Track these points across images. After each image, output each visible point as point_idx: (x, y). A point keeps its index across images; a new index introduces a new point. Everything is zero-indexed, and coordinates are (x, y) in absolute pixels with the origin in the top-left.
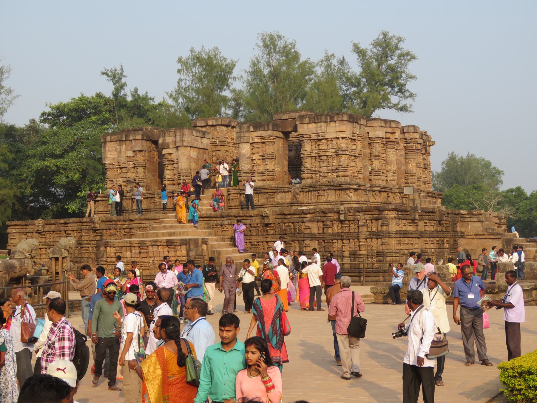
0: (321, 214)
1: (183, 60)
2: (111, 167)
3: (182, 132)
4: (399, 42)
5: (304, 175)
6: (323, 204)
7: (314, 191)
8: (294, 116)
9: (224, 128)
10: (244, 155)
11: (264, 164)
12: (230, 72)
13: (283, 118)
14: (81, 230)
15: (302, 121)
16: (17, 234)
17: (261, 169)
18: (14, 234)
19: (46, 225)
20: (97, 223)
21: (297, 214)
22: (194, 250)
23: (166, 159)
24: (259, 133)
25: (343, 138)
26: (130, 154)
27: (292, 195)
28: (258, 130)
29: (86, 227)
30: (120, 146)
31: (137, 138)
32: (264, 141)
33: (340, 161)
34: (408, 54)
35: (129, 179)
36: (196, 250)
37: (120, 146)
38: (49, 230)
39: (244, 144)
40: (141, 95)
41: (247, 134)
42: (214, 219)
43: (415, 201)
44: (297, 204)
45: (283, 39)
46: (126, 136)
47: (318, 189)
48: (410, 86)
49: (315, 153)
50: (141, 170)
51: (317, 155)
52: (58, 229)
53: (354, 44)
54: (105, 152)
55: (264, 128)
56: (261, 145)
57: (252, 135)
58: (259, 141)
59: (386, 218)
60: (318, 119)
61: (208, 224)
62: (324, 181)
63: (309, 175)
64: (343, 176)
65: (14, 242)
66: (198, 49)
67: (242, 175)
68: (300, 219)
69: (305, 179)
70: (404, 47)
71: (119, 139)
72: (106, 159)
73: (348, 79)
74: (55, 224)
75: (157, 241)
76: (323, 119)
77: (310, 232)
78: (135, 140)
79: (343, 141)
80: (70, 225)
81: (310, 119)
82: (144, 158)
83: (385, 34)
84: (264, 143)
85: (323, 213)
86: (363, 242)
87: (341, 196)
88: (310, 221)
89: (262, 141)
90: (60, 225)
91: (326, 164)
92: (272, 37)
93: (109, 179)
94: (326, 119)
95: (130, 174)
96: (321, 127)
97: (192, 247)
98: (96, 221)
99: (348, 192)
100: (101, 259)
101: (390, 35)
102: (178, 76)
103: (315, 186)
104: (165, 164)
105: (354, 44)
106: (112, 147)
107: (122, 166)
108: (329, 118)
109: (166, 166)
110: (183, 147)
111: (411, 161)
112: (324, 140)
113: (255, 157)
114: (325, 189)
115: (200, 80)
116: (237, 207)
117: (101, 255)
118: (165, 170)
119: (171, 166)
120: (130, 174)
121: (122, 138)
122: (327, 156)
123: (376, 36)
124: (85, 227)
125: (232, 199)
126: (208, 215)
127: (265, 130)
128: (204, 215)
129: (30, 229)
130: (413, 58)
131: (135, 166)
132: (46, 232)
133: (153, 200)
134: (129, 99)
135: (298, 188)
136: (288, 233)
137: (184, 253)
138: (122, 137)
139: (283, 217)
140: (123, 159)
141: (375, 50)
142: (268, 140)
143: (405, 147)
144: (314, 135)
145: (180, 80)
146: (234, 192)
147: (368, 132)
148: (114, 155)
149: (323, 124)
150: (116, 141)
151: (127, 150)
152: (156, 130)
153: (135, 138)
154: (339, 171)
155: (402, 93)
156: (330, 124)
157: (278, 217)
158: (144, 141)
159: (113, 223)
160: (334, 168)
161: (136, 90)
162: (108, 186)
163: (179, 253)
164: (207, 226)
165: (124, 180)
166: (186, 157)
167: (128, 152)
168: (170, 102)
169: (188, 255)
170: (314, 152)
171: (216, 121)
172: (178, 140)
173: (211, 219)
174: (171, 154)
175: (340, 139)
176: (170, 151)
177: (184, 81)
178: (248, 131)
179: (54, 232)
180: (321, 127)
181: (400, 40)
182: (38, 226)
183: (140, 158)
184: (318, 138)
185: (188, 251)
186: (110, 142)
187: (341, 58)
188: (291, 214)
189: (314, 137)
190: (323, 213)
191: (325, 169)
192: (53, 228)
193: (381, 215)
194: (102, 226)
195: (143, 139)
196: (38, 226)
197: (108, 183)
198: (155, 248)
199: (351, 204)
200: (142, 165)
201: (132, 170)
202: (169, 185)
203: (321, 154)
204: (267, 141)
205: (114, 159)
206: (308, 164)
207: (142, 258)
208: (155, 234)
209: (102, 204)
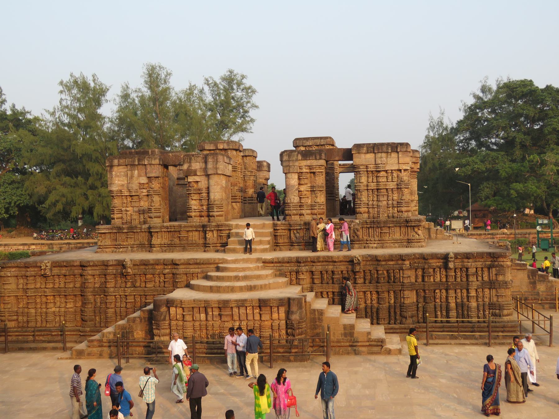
0: (420, 260)
1: (65, 82)
2: (118, 194)
3: (215, 158)
4: (243, 79)
6: (389, 242)
7: (378, 227)
8: (319, 142)
9: (234, 152)
10: (293, 186)
11: (314, 196)
12: (104, 95)
13: (305, 145)
14: (105, 275)
15: (360, 150)
16: (13, 278)
17: (310, 201)
18: (10, 278)
19: (54, 267)
20: (130, 267)
21: (392, 260)
22: (298, 312)
23: (192, 188)
24: (308, 162)
25: (404, 170)
26: (144, 180)
27: (352, 232)
28: (308, 159)
29: (113, 272)
30: (132, 170)
31: (153, 162)
32: (314, 171)
33: (403, 195)
34: (249, 88)
35: (142, 208)
36: (300, 313)
37: (132, 170)
38: (59, 274)
39: (293, 174)
40: (19, 110)
41: (297, 164)
42: (288, 265)
43: (431, 230)
44: (358, 242)
45: (165, 70)
46: (139, 160)
47: (382, 225)
48: (252, 113)
49: (373, 186)
50: (156, 199)
51: (375, 188)
52: (71, 273)
53: (205, 78)
54: (112, 177)
55: (315, 157)
56: (309, 175)
57: (300, 163)
58: (308, 171)
59: (502, 266)
60: (378, 149)
61: (280, 270)
62: (383, 217)
63: (367, 209)
65: (9, 287)
66: (77, 75)
67: (292, 209)
68: (397, 266)
69: (361, 213)
70: (247, 82)
71: (130, 163)
72: (113, 185)
73: (205, 105)
74: (67, 267)
75: (245, 300)
76: (385, 149)
77: (409, 281)
78: (150, 164)
79: (405, 173)
80: (89, 268)
81: (367, 148)
82: (159, 186)
84: (314, 173)
85: (424, 259)
86: (473, 293)
87: (407, 233)
88: (410, 269)
89: (312, 171)
90: (73, 268)
92: (153, 68)
93: (117, 208)
94: (388, 149)
95: (142, 203)
96: (381, 158)
97: (294, 308)
98: (128, 265)
99: (416, 230)
100: (162, 322)
101: (235, 72)
102: (59, 97)
103: (379, 223)
104: (191, 194)
105: (205, 78)
106: (120, 172)
107: (134, 194)
108: (390, 149)
109: (192, 195)
110: (216, 176)
112: (383, 172)
113: (302, 188)
115: (78, 100)
116: (285, 244)
117: (162, 318)
118: (190, 200)
119: (198, 195)
120: (142, 203)
121: (134, 162)
122: (387, 189)
123: (224, 72)
124: (111, 271)
125: (280, 235)
126: (280, 260)
127: (316, 159)
128: (275, 260)
129: (32, 272)
130: (254, 92)
131: (149, 194)
132: (54, 276)
133: (177, 235)
134: (9, 112)
135: (358, 224)
136: (383, 282)
137: (283, 315)
138: (134, 162)
139: (376, 263)
140: (135, 186)
141: (223, 83)
142: (319, 171)
144: (372, 166)
145: (61, 99)
146: (283, 228)
148: (123, 181)
149: (384, 155)
150: (126, 165)
151: (139, 176)
152: (171, 154)
153: (150, 162)
155: (244, 118)
156: (390, 155)
157: (368, 263)
158: (160, 166)
159: (150, 267)
160: (395, 203)
161: (14, 106)
162: (116, 216)
163: (275, 316)
164: (278, 273)
165: (136, 209)
166: (219, 187)
167: (141, 178)
168: (48, 117)
169: (287, 318)
170: (372, 184)
171: (228, 145)
172: (211, 167)
173: (283, 265)
174: (197, 182)
175: (402, 171)
176: (197, 178)
177: (65, 100)
178: (297, 160)
179: (65, 276)
180: (382, 158)
181: (243, 77)
182: (45, 269)
183: (156, 185)
184: (378, 169)
185: (288, 313)
186: (119, 165)
187: (201, 88)
188: (383, 261)
189: (372, 168)
190: (424, 259)
192: (64, 271)
193: (496, 263)
194: (134, 271)
195: (159, 164)
196: (45, 269)
197: (116, 212)
198: (242, 310)
199: (419, 242)
200: (159, 193)
201: (145, 198)
202: (195, 216)
203: (380, 187)
204: (318, 171)
205: (123, 185)
206: (364, 197)
208: (230, 288)
209: (109, 236)
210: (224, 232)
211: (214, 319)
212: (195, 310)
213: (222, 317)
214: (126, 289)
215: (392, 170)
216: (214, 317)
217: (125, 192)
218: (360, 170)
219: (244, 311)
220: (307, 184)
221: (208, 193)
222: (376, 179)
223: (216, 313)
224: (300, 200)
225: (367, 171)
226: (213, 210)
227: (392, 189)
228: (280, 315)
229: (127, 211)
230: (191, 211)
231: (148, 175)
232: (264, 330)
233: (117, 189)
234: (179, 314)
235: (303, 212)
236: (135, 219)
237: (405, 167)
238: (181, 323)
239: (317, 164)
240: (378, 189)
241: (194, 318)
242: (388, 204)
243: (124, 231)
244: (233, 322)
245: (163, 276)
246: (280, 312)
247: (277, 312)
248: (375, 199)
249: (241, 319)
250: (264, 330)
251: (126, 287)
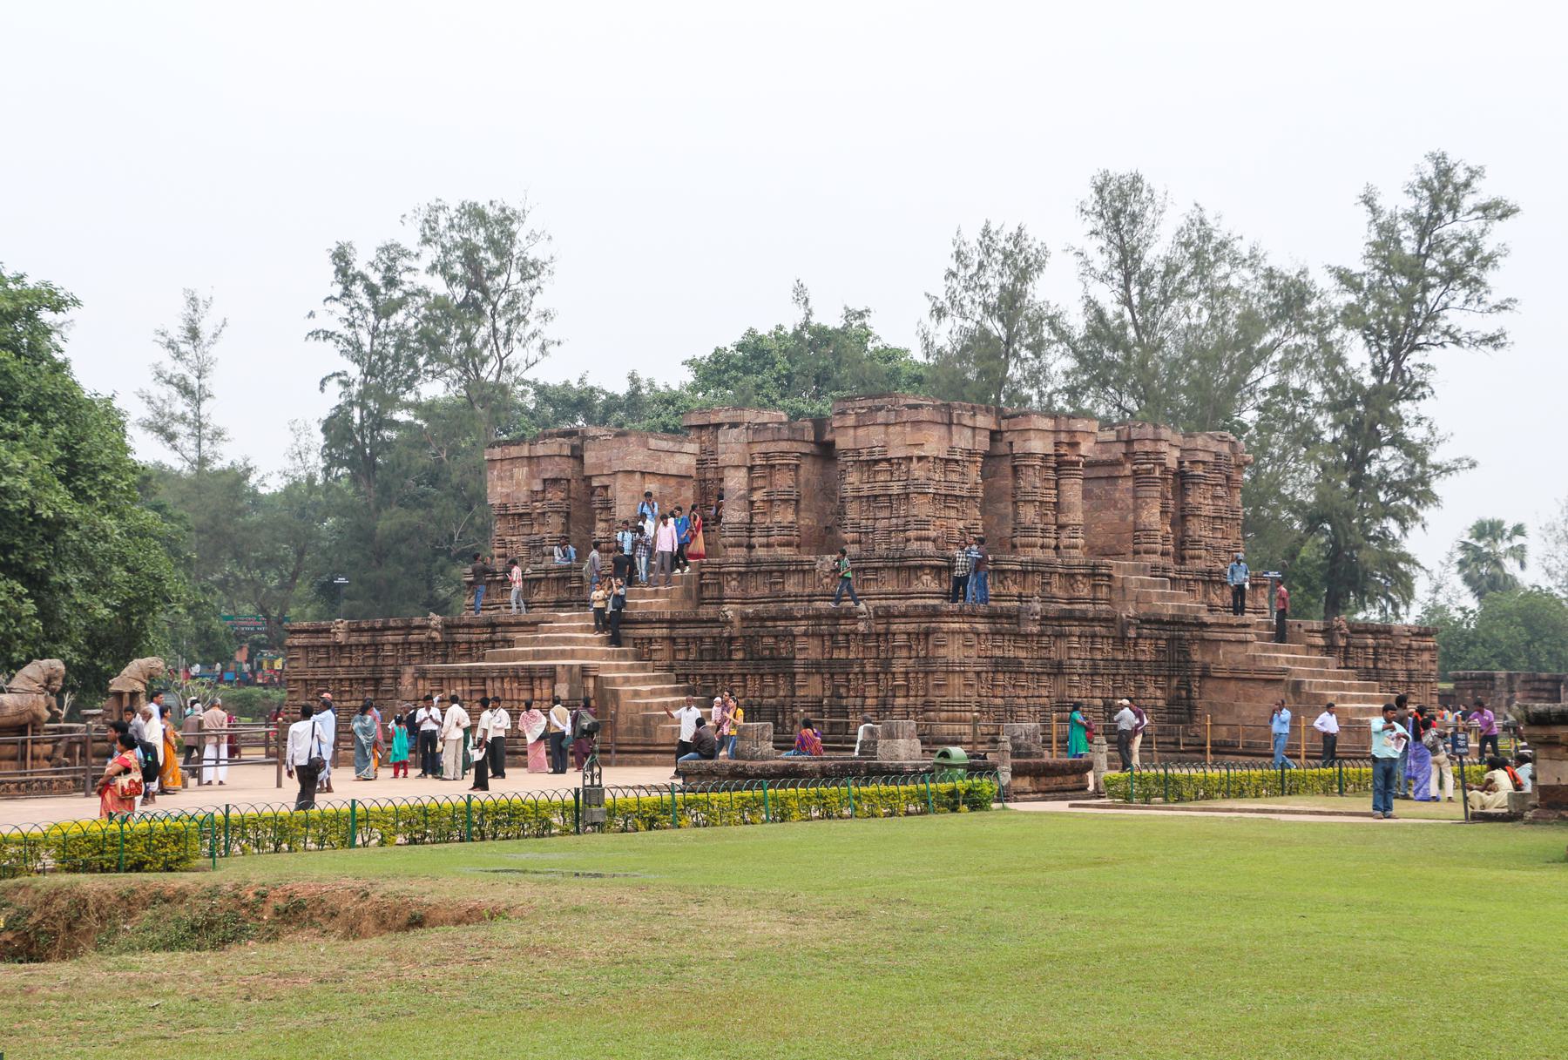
20: (436, 630)
25: (920, 459)
64: (919, 539)
83: (1438, 159)
84: (773, 466)
91: (886, 513)
111: (1147, 504)
114: (876, 565)
143: (1134, 471)
147: (1011, 443)
170: (866, 486)
191: (884, 523)
205: (508, 495)
224: (751, 518)
229: (512, 542)
235: (754, 540)
237: (917, 452)
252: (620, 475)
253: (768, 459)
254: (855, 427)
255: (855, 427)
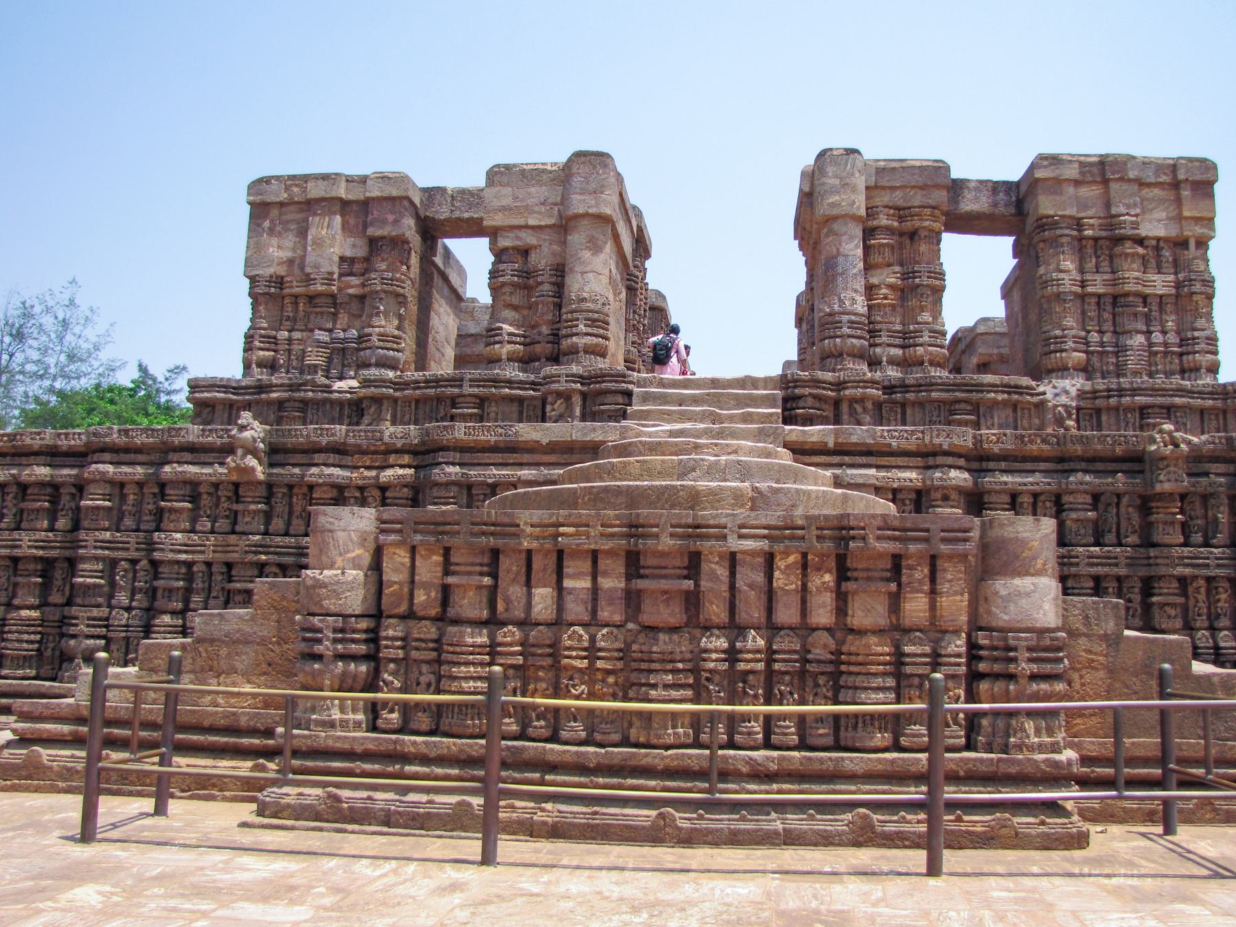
5: (1064, 354)
20: (254, 452)
51: (1110, 290)
58: (896, 224)
122: (1145, 298)
137: (954, 604)
154: (1197, 348)
163: (916, 607)
170: (1098, 277)
197: (257, 344)
203: (1127, 288)
207: (652, 629)
210: (610, 399)
211: (604, 614)
212: (505, 563)
213: (647, 606)
214: (233, 539)
215: (1158, 239)
216: (602, 603)
217: (295, 283)
218: (1058, 232)
219: (760, 578)
220: (889, 265)
221: (559, 288)
222: (1106, 263)
223: (612, 582)
225: (1081, 239)
226: (574, 330)
227: (1161, 296)
228: (944, 601)
230: (497, 338)
231: (371, 231)
232: (859, 681)
233: (271, 270)
234: (426, 586)
236: (316, 366)
238: (428, 630)
239: (927, 201)
240: (1115, 298)
241: (500, 606)
242: (1151, 345)
243: (274, 395)
244: (697, 632)
245: (377, 493)
246: (944, 587)
247: (926, 588)
248: (1108, 326)
249: (743, 616)
250: (859, 681)
251: (233, 532)
252: (585, 222)
253: (901, 219)
254: (1077, 183)
255: (1077, 183)
